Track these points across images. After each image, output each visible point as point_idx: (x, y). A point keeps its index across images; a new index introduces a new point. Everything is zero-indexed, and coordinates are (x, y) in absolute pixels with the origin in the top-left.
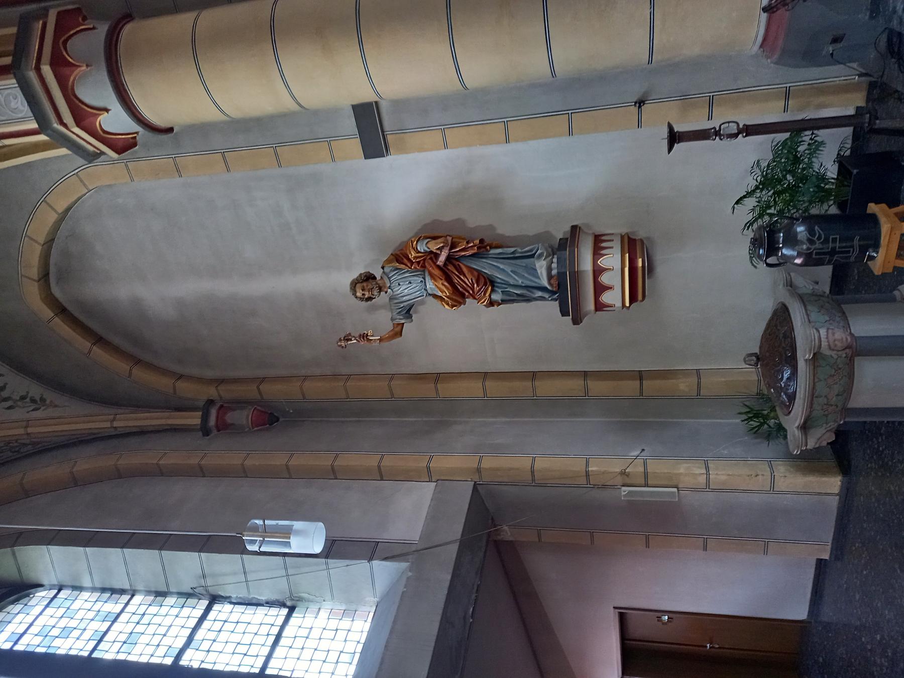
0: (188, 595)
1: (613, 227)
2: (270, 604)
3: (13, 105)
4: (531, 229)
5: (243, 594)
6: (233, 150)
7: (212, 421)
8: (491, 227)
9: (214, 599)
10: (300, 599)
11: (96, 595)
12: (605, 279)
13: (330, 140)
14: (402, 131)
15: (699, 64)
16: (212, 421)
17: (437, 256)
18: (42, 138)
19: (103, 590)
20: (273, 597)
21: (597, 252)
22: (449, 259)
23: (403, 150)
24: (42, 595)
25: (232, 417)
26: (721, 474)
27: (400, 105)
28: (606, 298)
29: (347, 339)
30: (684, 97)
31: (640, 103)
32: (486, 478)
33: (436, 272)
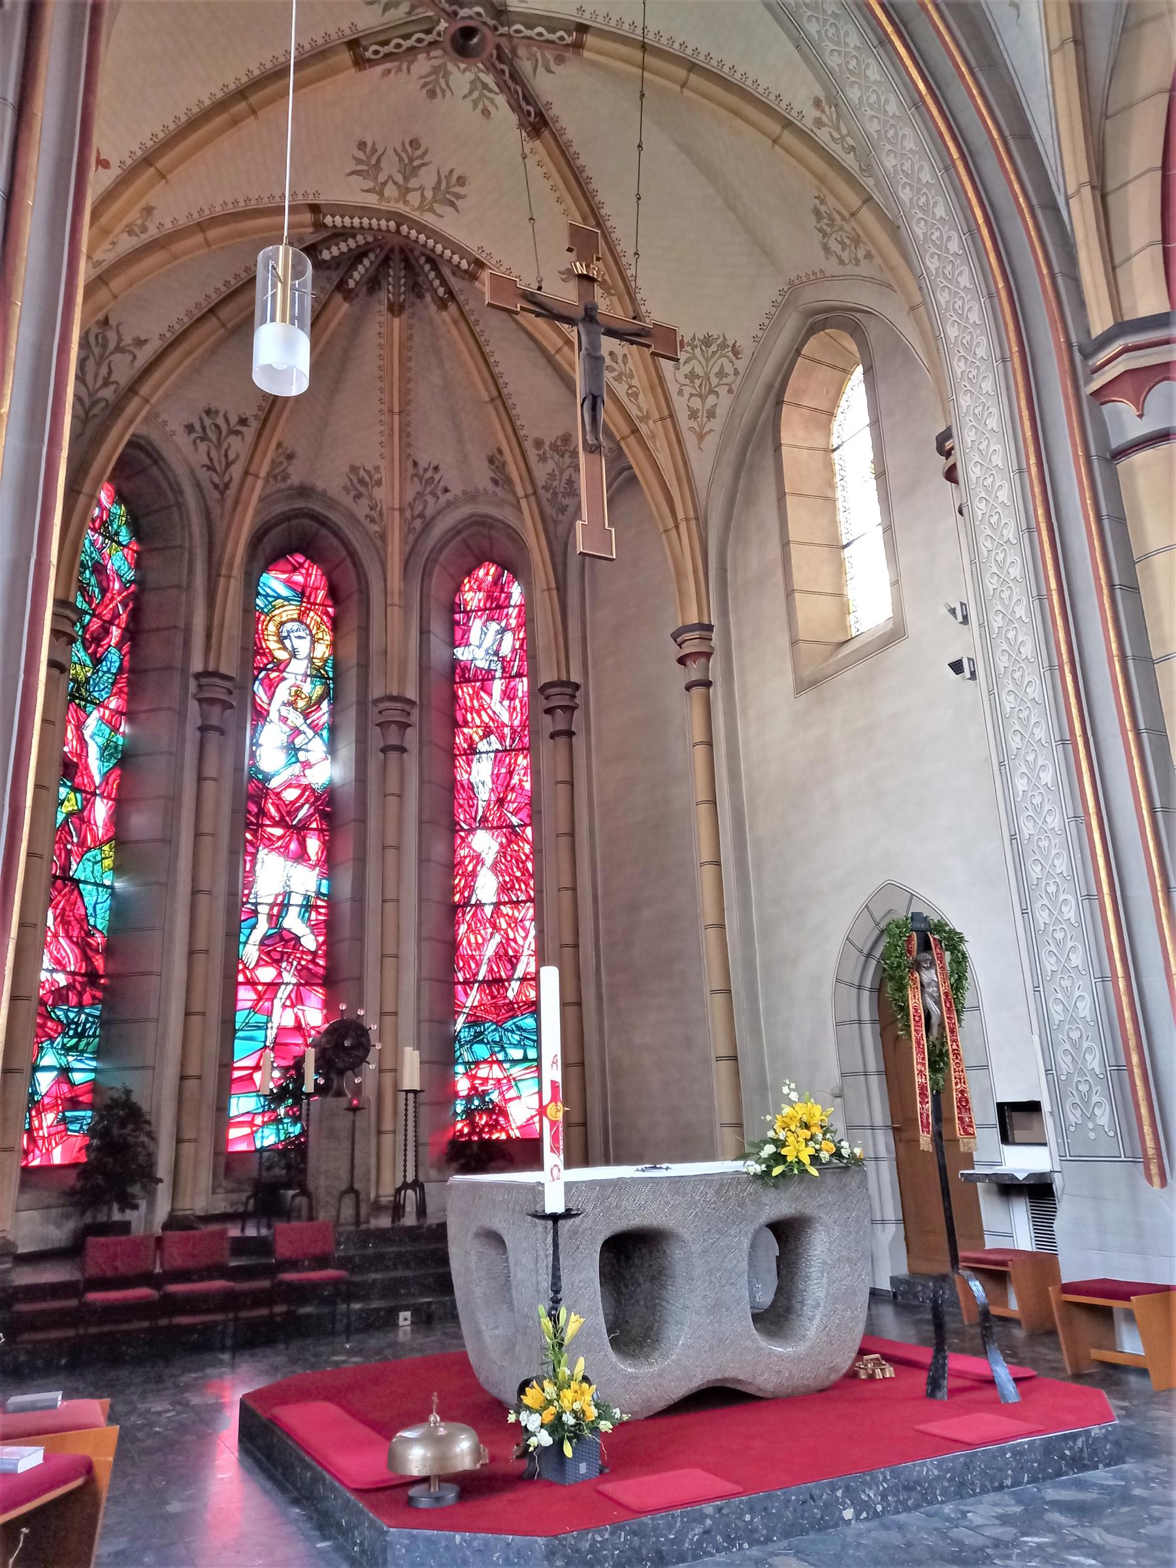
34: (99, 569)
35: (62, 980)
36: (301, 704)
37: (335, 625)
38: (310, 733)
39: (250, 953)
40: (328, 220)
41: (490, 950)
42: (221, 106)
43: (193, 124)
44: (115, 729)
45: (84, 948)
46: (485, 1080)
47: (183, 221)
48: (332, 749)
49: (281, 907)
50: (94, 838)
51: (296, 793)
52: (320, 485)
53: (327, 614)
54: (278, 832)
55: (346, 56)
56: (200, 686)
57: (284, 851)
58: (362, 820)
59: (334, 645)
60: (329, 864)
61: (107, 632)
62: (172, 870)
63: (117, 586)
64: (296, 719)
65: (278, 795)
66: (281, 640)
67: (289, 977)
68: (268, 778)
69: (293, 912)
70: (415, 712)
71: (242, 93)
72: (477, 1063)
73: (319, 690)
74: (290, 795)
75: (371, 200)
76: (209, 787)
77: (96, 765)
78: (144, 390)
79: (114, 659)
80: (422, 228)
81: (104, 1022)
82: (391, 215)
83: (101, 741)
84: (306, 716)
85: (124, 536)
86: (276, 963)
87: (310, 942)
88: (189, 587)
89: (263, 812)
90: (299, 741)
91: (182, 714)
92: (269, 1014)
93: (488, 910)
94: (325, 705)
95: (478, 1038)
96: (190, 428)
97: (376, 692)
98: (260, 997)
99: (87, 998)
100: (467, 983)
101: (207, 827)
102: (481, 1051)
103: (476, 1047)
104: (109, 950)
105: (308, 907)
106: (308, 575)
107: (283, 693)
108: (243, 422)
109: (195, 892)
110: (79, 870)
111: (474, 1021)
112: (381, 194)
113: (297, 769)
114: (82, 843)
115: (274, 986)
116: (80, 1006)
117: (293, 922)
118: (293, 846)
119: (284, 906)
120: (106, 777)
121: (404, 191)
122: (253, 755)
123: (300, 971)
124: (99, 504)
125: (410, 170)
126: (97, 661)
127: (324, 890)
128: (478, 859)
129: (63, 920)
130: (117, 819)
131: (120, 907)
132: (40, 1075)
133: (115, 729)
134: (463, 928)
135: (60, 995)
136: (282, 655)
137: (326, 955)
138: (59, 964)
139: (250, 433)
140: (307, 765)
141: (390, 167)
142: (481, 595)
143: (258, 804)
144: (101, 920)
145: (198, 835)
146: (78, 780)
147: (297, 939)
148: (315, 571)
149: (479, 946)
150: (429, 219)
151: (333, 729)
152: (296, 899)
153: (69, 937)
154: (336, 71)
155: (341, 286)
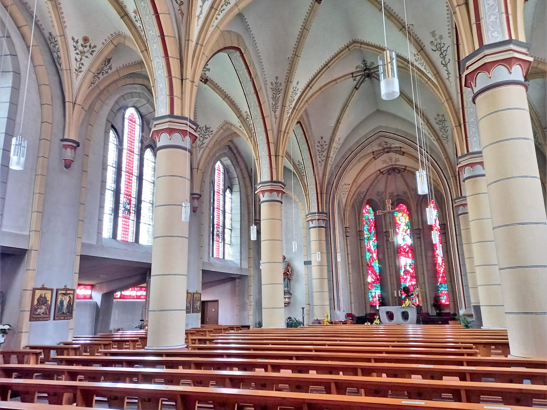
0: (231, 225)
1: (291, 301)
2: (231, 241)
3: (314, 210)
4: (292, 287)
5: (232, 236)
6: (306, 239)
7: (257, 221)
8: (292, 280)
9: (231, 230)
10: (232, 246)
11: (230, 206)
13: (307, 255)
14: (308, 268)
15: (313, 313)
16: (257, 221)
17: (288, 272)
19: (232, 208)
20: (232, 241)
21: (288, 298)
22: (288, 274)
23: (305, 267)
24: (230, 195)
26: (251, 317)
27: (311, 268)
30: (309, 311)
31: (309, 304)
32: (249, 278)
33: (286, 271)
34: (369, 219)
35: (373, 280)
36: (405, 231)
37: (409, 215)
39: (402, 274)
40: (382, 171)
41: (442, 271)
42: (361, 171)
43: (358, 174)
44: (375, 243)
45: (375, 275)
46: (444, 294)
47: (362, 182)
49: (405, 266)
50: (375, 260)
51: (406, 246)
52: (400, 194)
54: (404, 253)
55: (373, 159)
56: (385, 234)
57: (405, 257)
58: (415, 251)
60: (414, 258)
61: (371, 228)
62: (385, 264)
63: (371, 220)
64: (404, 234)
65: (403, 247)
66: (399, 220)
67: (409, 278)
68: (401, 245)
70: (422, 231)
71: (363, 168)
72: (442, 291)
73: (408, 228)
74: (405, 247)
75: (387, 165)
76: (389, 250)
77: (373, 249)
78: (365, 198)
79: (373, 232)
80: (396, 165)
81: (381, 285)
82: (390, 165)
83: (373, 245)
84: (406, 232)
85: (372, 212)
86: (406, 275)
87: (412, 271)
88: (382, 219)
89: (401, 251)
90: (405, 237)
91: (383, 239)
92: (406, 283)
93: (441, 264)
95: (442, 286)
96: (376, 195)
97: (415, 228)
98: (405, 280)
99: (378, 282)
100: (439, 277)
101: (389, 256)
102: (443, 289)
103: (442, 288)
104: (380, 275)
105: (410, 265)
106: (403, 207)
107: (401, 229)
108: (383, 192)
109: (389, 266)
110: (373, 264)
111: (441, 284)
112: (388, 164)
113: (405, 242)
114: (373, 261)
115: (406, 279)
116: (377, 284)
117: (408, 268)
118: (407, 255)
119: (406, 266)
120: (375, 250)
121: (391, 162)
122: (397, 241)
123: (411, 276)
124: (367, 209)
125: (391, 159)
126: (370, 233)
127: (413, 262)
128: (438, 255)
129: (372, 272)
130: (377, 256)
131: (380, 269)
132: (372, 293)
133: (375, 243)
134: (437, 267)
135: (374, 282)
136: (400, 223)
137: (415, 273)
138: (372, 278)
139: (384, 193)
141: (388, 161)
142: (433, 205)
143: (400, 249)
144: (377, 271)
145: (388, 257)
146: (371, 252)
148: (404, 206)
149: (440, 271)
150: (396, 163)
153: (373, 274)
154: (373, 162)
155: (389, 174)
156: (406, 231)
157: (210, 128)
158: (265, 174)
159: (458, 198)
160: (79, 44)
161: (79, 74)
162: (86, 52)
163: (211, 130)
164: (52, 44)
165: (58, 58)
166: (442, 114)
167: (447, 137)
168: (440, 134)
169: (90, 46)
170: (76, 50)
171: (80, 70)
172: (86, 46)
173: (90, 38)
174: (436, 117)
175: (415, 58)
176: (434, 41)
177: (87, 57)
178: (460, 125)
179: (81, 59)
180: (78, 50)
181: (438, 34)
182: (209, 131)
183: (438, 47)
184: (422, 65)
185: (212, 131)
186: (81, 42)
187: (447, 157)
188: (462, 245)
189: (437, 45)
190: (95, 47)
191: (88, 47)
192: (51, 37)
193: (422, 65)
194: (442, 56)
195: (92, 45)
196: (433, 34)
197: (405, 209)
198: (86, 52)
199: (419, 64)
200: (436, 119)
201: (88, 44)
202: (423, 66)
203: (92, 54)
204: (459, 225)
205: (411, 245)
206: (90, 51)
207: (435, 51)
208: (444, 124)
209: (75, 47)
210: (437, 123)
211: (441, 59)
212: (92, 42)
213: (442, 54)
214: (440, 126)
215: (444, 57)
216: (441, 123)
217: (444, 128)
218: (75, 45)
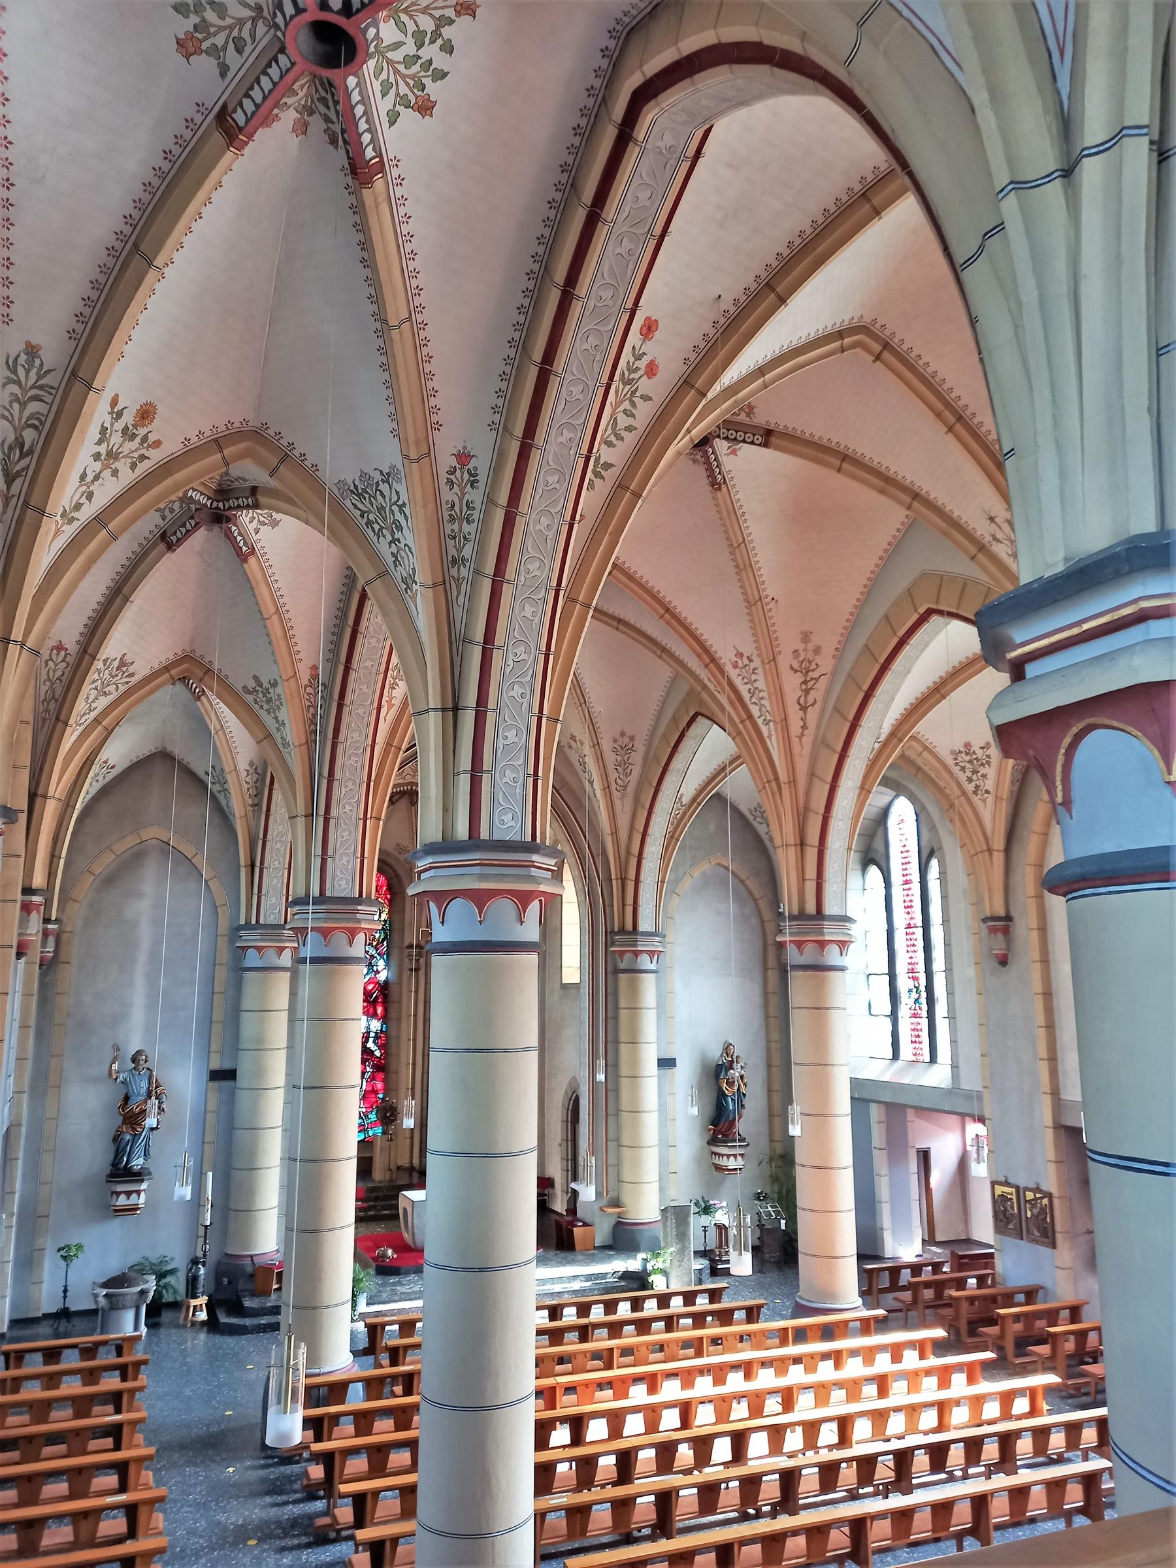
12: (134, 1196)
18: (254, 922)
25: (51, 940)
27: (232, 1093)
28: (122, 1198)
29: (118, 1049)
36: (375, 944)
38: (378, 957)
48: (387, 965)
53: (386, 898)
59: (389, 913)
69: (371, 1040)
73: (382, 937)
82: (408, 784)
94: (385, 943)
105: (377, 1037)
118: (371, 1010)
123: (375, 1067)
140: (378, 972)
147: (373, 1052)
151: (388, 953)
152: (372, 1035)
156: (378, 944)
157: (133, 663)
158: (342, 872)
159: (622, 931)
160: (119, 426)
161: (65, 528)
162: (123, 457)
163: (131, 669)
164: (15, 389)
165: (10, 448)
166: (631, 734)
167: (626, 787)
168: (613, 775)
169: (145, 439)
170: (99, 443)
171: (73, 514)
172: (133, 437)
173: (161, 410)
174: (617, 736)
175: (739, 661)
176: (801, 651)
177: (115, 473)
178: (802, 844)
179: (97, 477)
180: (104, 445)
181: (815, 640)
182: (124, 672)
183: (803, 666)
184: (745, 680)
185: (132, 675)
186: (128, 418)
187: (615, 833)
188: (617, 1042)
189: (802, 662)
190: (157, 444)
191: (138, 439)
192: (30, 363)
193: (745, 680)
194: (804, 687)
195: (152, 438)
196: (806, 637)
197: (382, 887)
198: (123, 457)
199: (739, 675)
200: (615, 741)
201: (142, 431)
202: (749, 686)
203: (133, 466)
204: (616, 994)
205: (386, 982)
206: (136, 455)
207: (796, 671)
208: (628, 756)
209: (103, 430)
210: (615, 750)
211: (799, 693)
212: (156, 429)
213: (805, 682)
214: (619, 758)
215: (807, 692)
216: (623, 752)
217: (624, 765)
218: (107, 425)
